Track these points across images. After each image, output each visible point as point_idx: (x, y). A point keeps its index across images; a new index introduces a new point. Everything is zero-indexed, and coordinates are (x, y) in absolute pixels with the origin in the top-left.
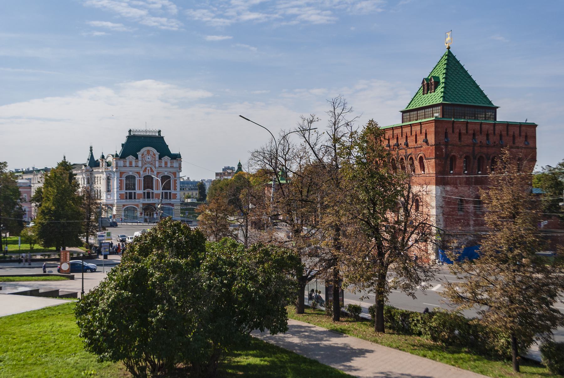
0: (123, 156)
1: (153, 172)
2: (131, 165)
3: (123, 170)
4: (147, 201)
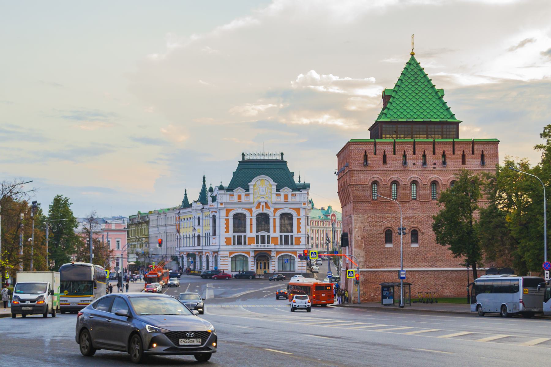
0: (230, 189)
1: (269, 208)
2: (240, 202)
3: (229, 207)
4: (260, 247)
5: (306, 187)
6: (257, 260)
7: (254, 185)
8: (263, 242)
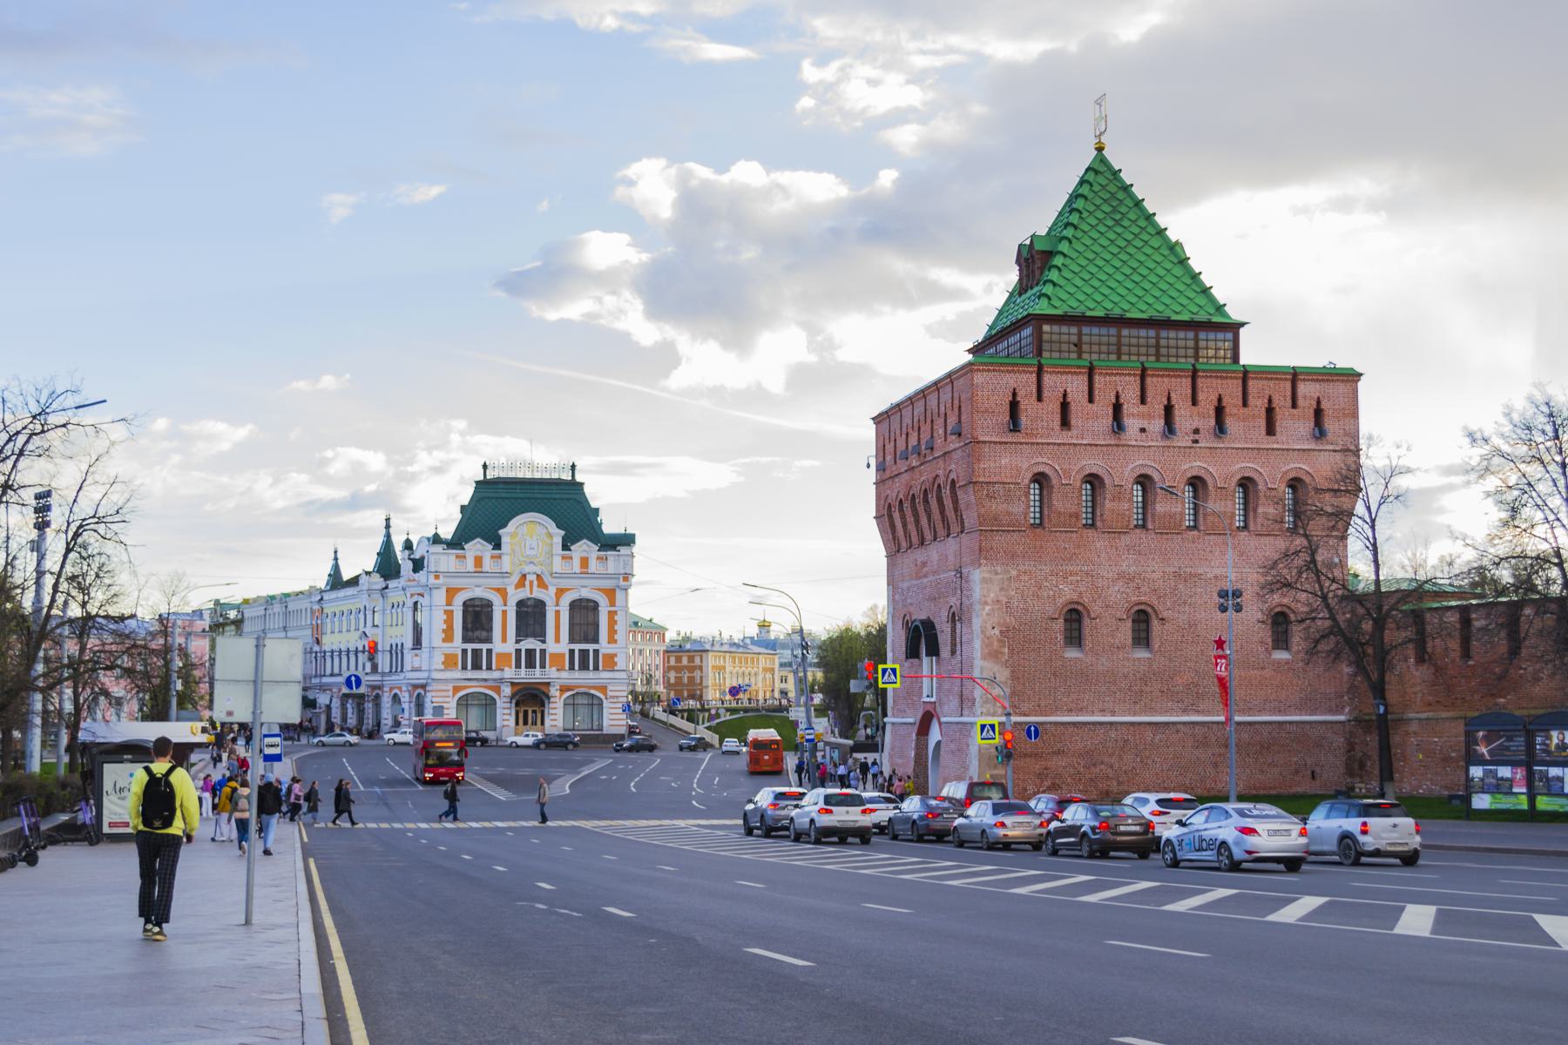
0: (457, 542)
1: (546, 587)
3: (455, 583)
4: (524, 675)
5: (627, 540)
6: (517, 705)
7: (512, 535)
8: (531, 664)
